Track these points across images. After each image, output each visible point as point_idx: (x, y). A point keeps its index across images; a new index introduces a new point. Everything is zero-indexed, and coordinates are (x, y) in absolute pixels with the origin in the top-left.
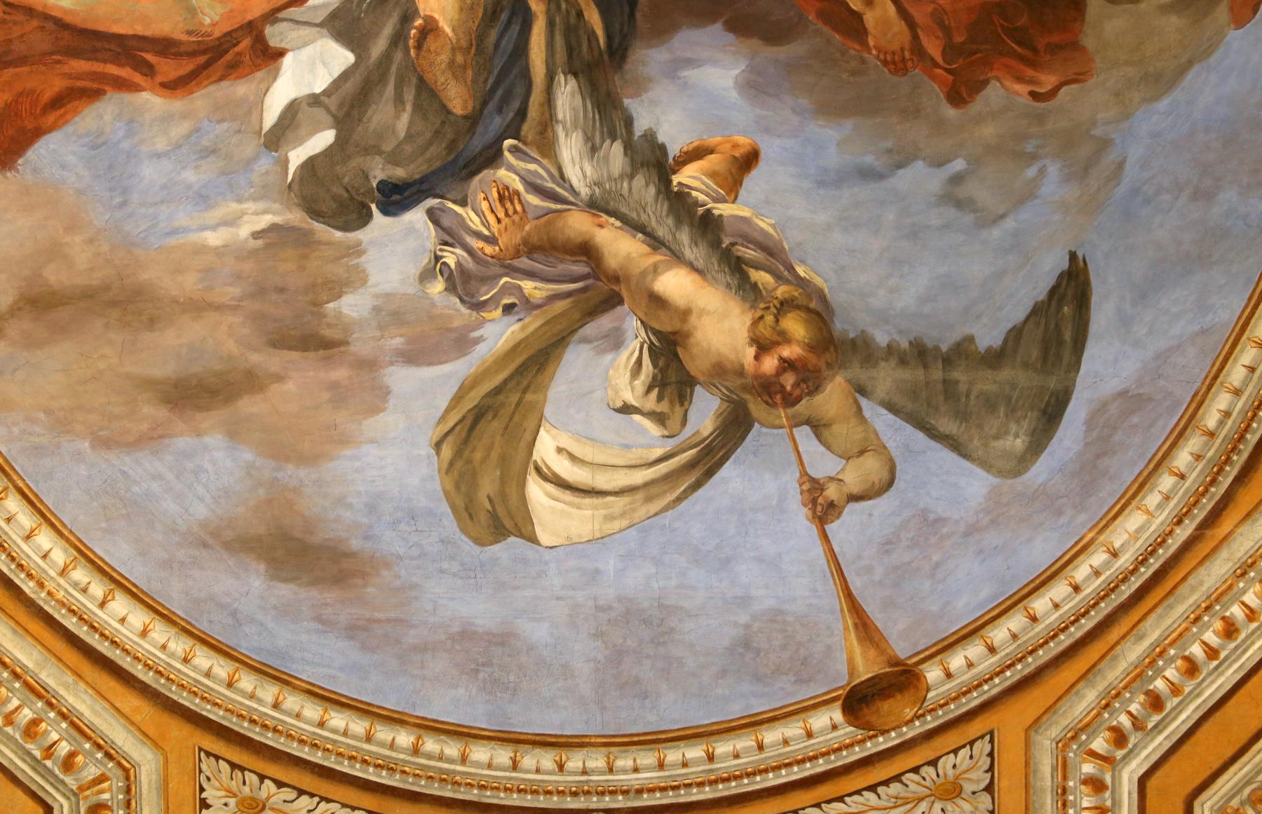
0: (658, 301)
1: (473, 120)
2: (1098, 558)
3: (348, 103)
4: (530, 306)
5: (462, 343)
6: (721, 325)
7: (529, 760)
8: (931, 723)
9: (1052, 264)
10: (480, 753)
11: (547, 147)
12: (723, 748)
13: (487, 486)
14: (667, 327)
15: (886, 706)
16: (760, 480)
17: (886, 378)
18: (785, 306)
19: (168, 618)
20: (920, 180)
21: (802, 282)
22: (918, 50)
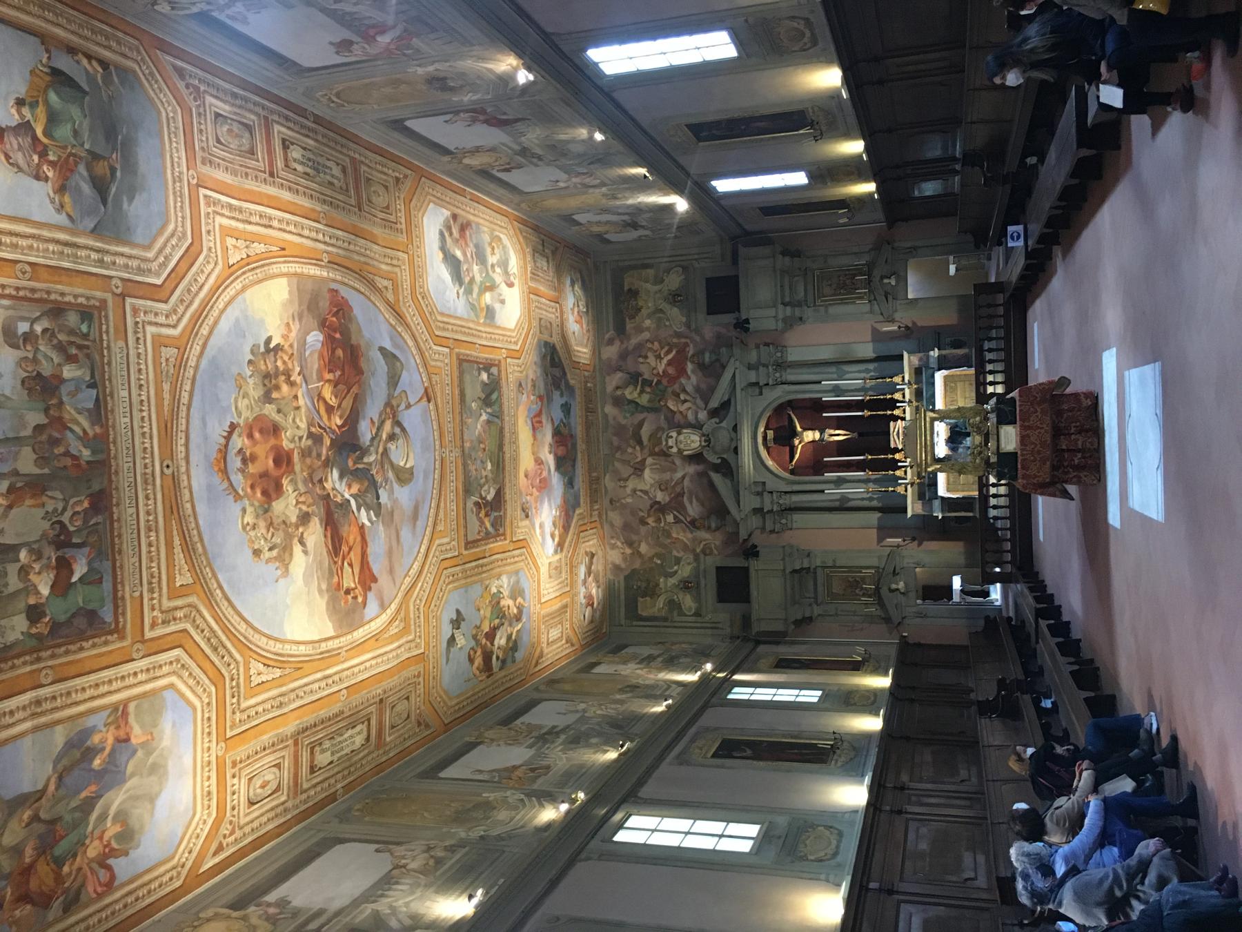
3: (368, 509)
11: (370, 464)
13: (407, 476)
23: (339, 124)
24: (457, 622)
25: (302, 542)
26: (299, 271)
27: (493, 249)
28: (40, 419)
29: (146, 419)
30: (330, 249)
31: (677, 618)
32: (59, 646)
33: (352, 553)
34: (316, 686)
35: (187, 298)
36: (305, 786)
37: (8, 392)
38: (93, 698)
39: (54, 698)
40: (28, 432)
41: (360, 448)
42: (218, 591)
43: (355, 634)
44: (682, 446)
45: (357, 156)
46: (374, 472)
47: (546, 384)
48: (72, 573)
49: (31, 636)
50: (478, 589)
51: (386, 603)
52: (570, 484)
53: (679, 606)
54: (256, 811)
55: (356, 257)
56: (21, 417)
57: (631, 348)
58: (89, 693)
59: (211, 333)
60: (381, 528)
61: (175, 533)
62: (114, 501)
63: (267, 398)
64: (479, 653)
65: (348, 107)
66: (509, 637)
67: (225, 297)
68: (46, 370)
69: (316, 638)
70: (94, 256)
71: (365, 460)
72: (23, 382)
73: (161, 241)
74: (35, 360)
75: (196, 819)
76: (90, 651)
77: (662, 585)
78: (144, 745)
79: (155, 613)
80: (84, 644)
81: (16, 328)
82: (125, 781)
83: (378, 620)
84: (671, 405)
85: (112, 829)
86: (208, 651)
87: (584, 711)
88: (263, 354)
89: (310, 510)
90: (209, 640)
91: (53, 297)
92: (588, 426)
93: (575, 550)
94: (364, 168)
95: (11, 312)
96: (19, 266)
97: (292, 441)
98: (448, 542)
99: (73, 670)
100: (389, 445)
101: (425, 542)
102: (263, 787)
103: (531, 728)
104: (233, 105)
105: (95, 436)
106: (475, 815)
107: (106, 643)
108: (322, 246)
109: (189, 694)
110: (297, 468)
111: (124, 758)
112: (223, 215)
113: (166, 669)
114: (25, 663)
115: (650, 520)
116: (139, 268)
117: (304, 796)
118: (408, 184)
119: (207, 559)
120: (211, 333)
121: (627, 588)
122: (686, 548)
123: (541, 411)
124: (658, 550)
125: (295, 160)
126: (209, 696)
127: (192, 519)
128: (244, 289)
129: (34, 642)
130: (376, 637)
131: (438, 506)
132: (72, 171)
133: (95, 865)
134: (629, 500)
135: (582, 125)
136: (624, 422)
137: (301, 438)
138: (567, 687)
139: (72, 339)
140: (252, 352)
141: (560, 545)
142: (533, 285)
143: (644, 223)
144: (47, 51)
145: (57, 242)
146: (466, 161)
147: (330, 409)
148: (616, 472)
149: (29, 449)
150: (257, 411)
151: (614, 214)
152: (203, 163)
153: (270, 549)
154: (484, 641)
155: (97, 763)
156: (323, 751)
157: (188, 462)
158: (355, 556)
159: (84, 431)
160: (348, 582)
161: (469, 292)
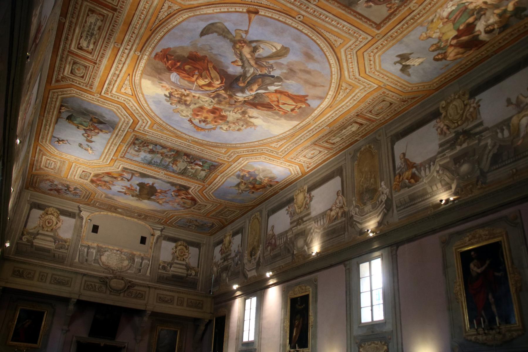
0: (252, 56)
1: (260, 78)
2: (215, 11)
3: (272, 84)
4: (266, 62)
5: (276, 63)
6: (246, 51)
7: (301, 29)
8: (249, 6)
9: (204, 38)
10: (306, 32)
11: (254, 73)
12: (277, 17)
14: (252, 54)
15: (253, 10)
17: (230, 37)
18: (237, 49)
19: (328, 59)
20: (214, 52)
21: (234, 49)
22: (208, 62)
25: (251, 117)
30: (134, 48)
55: (143, 30)
60: (288, 82)
83: (323, 104)
89: (243, 110)
108: (132, 52)
110: (222, 107)
128: (143, 94)
130: (330, 106)
137: (212, 102)
140: (168, 101)
147: (209, 85)
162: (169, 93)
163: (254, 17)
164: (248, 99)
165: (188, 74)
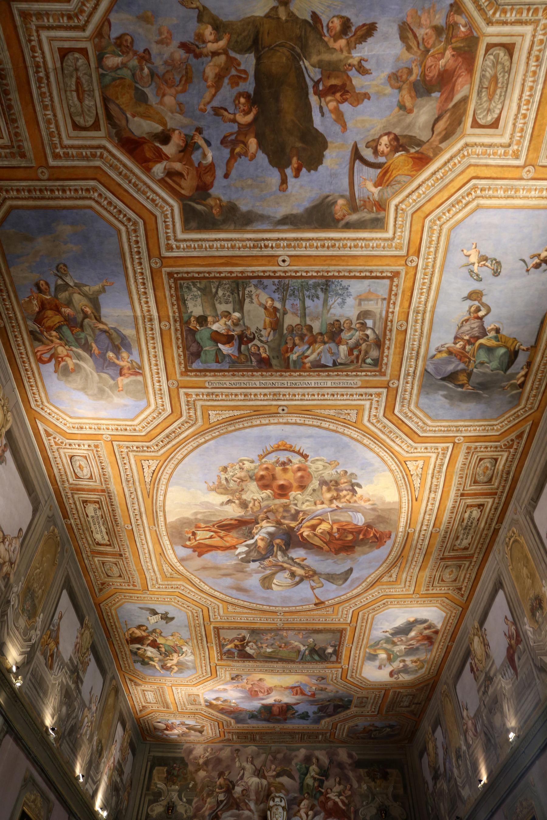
3: (247, 553)
6: (300, 572)
11: (276, 556)
13: (266, 585)
16: (305, 586)
23: (495, 547)
24: (166, 618)
25: (229, 502)
26: (403, 510)
27: (415, 662)
28: (316, 331)
29: (313, 398)
30: (417, 534)
31: (147, 798)
32: (182, 334)
33: (219, 539)
34: (136, 507)
35: (386, 431)
36: (76, 496)
37: (332, 311)
38: (149, 353)
39: (152, 329)
40: (308, 322)
41: (287, 550)
42: (203, 440)
43: (166, 538)
44: (274, 810)
45: (475, 559)
46: (271, 559)
47: (323, 700)
48: (224, 344)
49: (190, 318)
50: (185, 633)
51: (184, 563)
52: (253, 716)
53: (156, 801)
54: (66, 461)
55: (411, 554)
56: (317, 318)
57: (346, 771)
58: (152, 351)
59: (365, 445)
60: (234, 562)
61: (242, 412)
62: (264, 373)
63: (323, 483)
64: (144, 634)
65: (507, 550)
66: (151, 659)
67: (387, 458)
68: (345, 335)
69: (167, 509)
70: (411, 370)
71: (279, 553)
72: (338, 321)
73: (421, 415)
74: (350, 329)
75: (68, 419)
76: (176, 352)
77: (173, 787)
78: (117, 385)
79: (194, 396)
80: (181, 349)
81: (369, 319)
82: (97, 372)
83: (173, 556)
84: (305, 803)
85: (71, 363)
86: (167, 431)
87: (90, 709)
88: (351, 481)
89: (249, 509)
90: (174, 432)
91: (387, 342)
92: (292, 734)
93: (206, 717)
94: (467, 563)
95: (378, 316)
96: (405, 323)
97: (295, 499)
98: (220, 614)
99: (166, 342)
100: (288, 572)
101: (221, 596)
102: (80, 466)
103: (85, 665)
104: (503, 471)
105: (304, 363)
106: (29, 603)
107: (180, 363)
109: (143, 416)
110: (277, 501)
111: (111, 372)
112: (437, 459)
113: (159, 401)
114: (174, 312)
115: (221, 781)
116: (404, 399)
117: (70, 495)
118: (458, 597)
119: (224, 434)
120: (365, 445)
121: (175, 759)
122: (198, 809)
123: (305, 695)
124: (199, 786)
125: (471, 512)
126: (140, 431)
127: (250, 424)
128: (391, 470)
129: (185, 318)
130: (162, 554)
131: (244, 607)
132: (460, 360)
133: (52, 351)
134: (237, 764)
135: (519, 721)
136: (293, 763)
137: (296, 505)
138: (111, 701)
139: (363, 353)
140: (352, 474)
141: (210, 705)
142: (391, 693)
143: (438, 786)
144: (528, 349)
145: (419, 348)
146: (476, 639)
147: (313, 528)
148: (258, 755)
149: (299, 322)
150: (315, 475)
151: (445, 760)
152: (468, 448)
153: (226, 479)
154: (151, 638)
155: (111, 354)
156: (95, 510)
157: (285, 424)
158: (216, 541)
159: (307, 357)
160: (201, 535)
161: (388, 641)
162: (356, 492)
163: (315, 601)
164: (257, 528)
165: (345, 530)
